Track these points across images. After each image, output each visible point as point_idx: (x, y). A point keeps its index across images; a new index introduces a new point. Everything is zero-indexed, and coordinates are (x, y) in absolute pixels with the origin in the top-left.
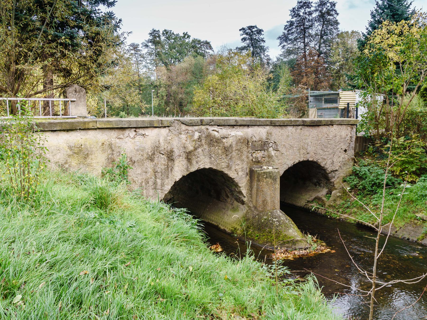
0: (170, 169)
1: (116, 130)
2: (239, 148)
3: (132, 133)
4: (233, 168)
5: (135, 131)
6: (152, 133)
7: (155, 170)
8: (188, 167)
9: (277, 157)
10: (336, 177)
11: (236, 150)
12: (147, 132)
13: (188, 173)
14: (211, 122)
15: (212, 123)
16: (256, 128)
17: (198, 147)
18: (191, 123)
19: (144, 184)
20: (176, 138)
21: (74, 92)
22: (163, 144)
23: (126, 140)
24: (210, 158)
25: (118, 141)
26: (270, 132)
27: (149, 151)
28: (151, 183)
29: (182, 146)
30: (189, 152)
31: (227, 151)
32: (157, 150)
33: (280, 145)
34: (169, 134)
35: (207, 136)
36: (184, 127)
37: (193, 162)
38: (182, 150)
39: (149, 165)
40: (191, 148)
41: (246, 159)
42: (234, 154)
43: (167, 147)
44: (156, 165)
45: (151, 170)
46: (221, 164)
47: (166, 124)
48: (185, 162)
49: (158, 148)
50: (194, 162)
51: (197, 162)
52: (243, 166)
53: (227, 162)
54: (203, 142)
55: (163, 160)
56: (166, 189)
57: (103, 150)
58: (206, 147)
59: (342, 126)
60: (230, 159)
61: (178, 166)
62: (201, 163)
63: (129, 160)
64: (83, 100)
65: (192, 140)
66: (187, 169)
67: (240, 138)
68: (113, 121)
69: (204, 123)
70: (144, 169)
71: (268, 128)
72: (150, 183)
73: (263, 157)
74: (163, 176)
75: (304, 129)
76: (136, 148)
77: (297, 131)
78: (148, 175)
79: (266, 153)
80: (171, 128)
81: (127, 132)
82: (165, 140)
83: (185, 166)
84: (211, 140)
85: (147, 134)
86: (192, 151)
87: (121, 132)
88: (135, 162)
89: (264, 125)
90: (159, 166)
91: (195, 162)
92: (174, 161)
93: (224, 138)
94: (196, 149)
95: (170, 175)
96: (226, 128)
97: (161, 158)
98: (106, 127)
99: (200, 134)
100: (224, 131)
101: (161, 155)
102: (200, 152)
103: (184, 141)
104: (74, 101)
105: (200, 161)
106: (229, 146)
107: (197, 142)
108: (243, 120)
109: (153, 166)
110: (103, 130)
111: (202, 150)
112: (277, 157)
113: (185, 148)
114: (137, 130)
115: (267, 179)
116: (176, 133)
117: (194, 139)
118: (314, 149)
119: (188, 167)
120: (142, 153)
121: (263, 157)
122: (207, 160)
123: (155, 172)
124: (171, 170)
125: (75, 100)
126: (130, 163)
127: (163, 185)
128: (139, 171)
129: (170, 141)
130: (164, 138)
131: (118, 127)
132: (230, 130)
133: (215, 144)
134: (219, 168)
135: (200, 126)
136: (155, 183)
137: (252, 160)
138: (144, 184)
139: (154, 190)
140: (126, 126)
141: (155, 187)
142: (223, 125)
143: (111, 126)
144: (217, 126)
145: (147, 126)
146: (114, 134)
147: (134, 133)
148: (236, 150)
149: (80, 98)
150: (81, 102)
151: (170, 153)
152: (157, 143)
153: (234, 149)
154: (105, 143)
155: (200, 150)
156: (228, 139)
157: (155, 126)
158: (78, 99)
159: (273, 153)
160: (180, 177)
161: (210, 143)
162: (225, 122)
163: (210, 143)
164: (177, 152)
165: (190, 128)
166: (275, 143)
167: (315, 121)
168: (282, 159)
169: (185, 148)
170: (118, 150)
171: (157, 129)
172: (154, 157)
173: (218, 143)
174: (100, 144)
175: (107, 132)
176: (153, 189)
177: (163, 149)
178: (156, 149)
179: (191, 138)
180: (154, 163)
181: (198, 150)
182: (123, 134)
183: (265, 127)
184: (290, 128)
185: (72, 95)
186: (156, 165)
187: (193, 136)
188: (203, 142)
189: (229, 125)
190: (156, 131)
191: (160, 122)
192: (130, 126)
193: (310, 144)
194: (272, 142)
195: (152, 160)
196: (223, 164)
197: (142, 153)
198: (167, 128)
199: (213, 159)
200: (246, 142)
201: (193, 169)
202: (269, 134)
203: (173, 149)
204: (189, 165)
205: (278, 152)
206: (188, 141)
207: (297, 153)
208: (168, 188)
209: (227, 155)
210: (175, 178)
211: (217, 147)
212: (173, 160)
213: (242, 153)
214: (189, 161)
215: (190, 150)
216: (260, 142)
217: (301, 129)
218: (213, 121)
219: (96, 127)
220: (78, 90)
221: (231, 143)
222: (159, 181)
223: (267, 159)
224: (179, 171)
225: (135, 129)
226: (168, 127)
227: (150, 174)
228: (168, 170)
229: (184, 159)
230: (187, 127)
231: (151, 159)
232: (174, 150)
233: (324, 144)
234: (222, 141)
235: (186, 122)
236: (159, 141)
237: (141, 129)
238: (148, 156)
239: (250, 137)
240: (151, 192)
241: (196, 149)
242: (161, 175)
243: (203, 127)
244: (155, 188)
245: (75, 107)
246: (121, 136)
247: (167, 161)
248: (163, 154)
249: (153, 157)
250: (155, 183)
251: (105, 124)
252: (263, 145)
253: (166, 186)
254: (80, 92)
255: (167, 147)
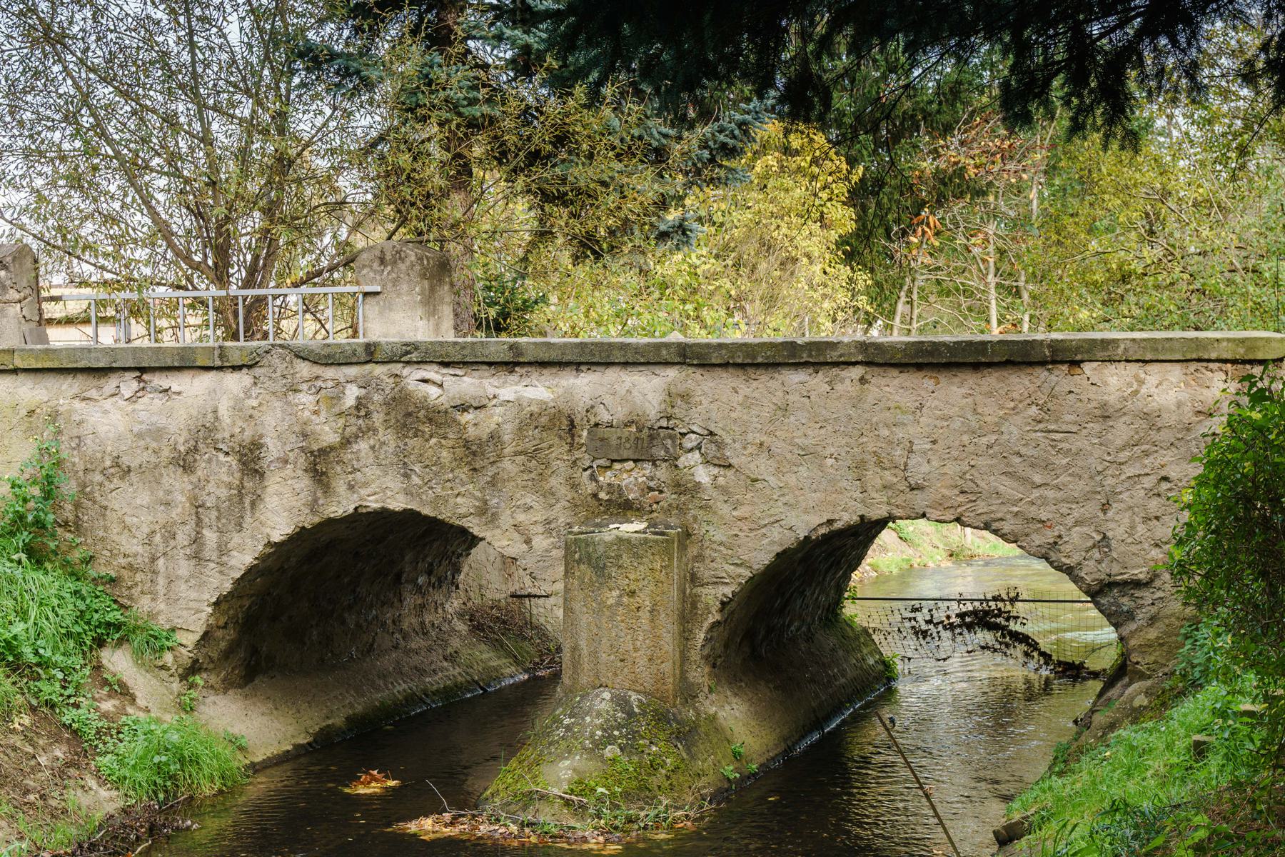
0: (247, 501)
1: (80, 377)
2: (530, 446)
3: (129, 385)
4: (505, 519)
5: (139, 379)
6: (194, 387)
7: (196, 499)
8: (316, 500)
9: (724, 490)
10: (1141, 616)
11: (517, 454)
12: (175, 382)
13: (317, 520)
14: (408, 353)
15: (414, 357)
16: (612, 374)
17: (357, 437)
18: (328, 356)
19: (158, 538)
20: (277, 404)
21: (376, 265)
22: (228, 421)
23: (108, 404)
24: (406, 476)
25: (78, 405)
26: (681, 388)
27: (181, 440)
28: (183, 537)
29: (297, 429)
30: (319, 450)
31: (474, 454)
32: (206, 439)
33: (738, 445)
34: (254, 392)
35: (394, 399)
36: (304, 369)
37: (334, 485)
38: (294, 441)
39: (179, 485)
40: (328, 435)
41: (563, 491)
42: (509, 466)
43: (243, 430)
44: (199, 486)
45: (184, 499)
46: (452, 501)
47: (236, 359)
48: (305, 482)
49: (210, 431)
50: (340, 486)
51: (351, 487)
52: (552, 514)
53: (478, 494)
54: (378, 418)
55: (224, 469)
56: (233, 562)
57: (29, 429)
58: (388, 437)
59: (1150, 367)
60: (492, 483)
61: (279, 494)
62: (369, 491)
63: (108, 463)
64: (405, 287)
65: (336, 410)
66: (313, 506)
67: (534, 408)
68: (61, 350)
69: (378, 357)
70: (161, 494)
71: (672, 373)
72: (180, 537)
73: (651, 489)
74: (224, 521)
75: (883, 382)
76: (136, 430)
77: (839, 387)
78: (175, 513)
79: (663, 473)
80: (257, 371)
81: (111, 383)
82: (237, 408)
83: (305, 497)
84: (410, 414)
85: (175, 388)
86: (332, 448)
87: (91, 381)
88: (129, 471)
89: (648, 363)
90: (211, 487)
91: (345, 487)
92: (262, 475)
93: (464, 408)
94: (349, 442)
95: (248, 519)
96: (476, 374)
97: (219, 463)
98: (39, 366)
99: (363, 391)
100: (467, 385)
101: (221, 457)
102: (363, 454)
103: (307, 413)
104: (378, 293)
105: (366, 484)
106: (485, 437)
107: (353, 420)
108: (549, 345)
109: (190, 487)
110: (40, 376)
111: (372, 448)
112: (724, 490)
113: (305, 436)
114: (145, 377)
115: (582, 567)
116: (278, 387)
117: (344, 408)
118: (952, 469)
119: (316, 500)
120: (154, 445)
121: (651, 489)
122: (393, 482)
123: (198, 507)
124: (253, 504)
125: (378, 289)
126: (112, 470)
127: (223, 550)
128: (144, 498)
129: (255, 413)
130: (232, 403)
131: (75, 366)
132: (494, 381)
133: (427, 429)
134: (445, 514)
135: (368, 367)
136: (197, 540)
137: (595, 496)
138: (158, 538)
139: (193, 562)
140: (101, 365)
141: (196, 553)
142: (465, 363)
143: (56, 365)
144: (435, 367)
145: (169, 364)
146: (70, 386)
147: (135, 385)
148: (517, 454)
149: (395, 282)
150: (399, 295)
151: (251, 450)
152: (210, 416)
153: (509, 450)
154: (38, 411)
155: (363, 446)
156: (481, 414)
157: (198, 364)
158: (389, 285)
159: (703, 475)
160: (289, 530)
161: (405, 425)
162: (465, 352)
163: (405, 425)
164: (273, 448)
165: (330, 373)
166: (711, 433)
167: (944, 344)
168: (752, 504)
169: (305, 436)
170: (75, 432)
171: (212, 374)
172: (195, 461)
173: (439, 425)
174: (24, 412)
175: (52, 382)
176: (189, 558)
177: (227, 435)
178: (205, 434)
179: (333, 406)
180: (194, 479)
181: (355, 447)
182: (99, 388)
183: (657, 370)
184: (794, 378)
185: (372, 275)
186: (199, 486)
187: (339, 398)
188: (378, 418)
189: (490, 364)
190: (205, 381)
191: (217, 353)
192: (114, 365)
193: (922, 445)
194: (695, 428)
195: (187, 468)
196: (459, 500)
197: (154, 445)
198: (245, 370)
199: (415, 480)
200: (565, 424)
201: (341, 505)
202: (674, 397)
203: (261, 436)
204: (319, 494)
205: (730, 473)
206: (323, 414)
207: (844, 484)
208: (243, 558)
209: (475, 470)
210: (268, 530)
211: (434, 441)
212: (261, 474)
213: (548, 465)
214: (320, 481)
215: (325, 444)
216: (634, 429)
217: (862, 380)
218: (416, 349)
219: (11, 367)
220: (388, 257)
221: (493, 426)
222: (210, 536)
223: (669, 497)
224: (281, 513)
225: (138, 374)
226: (249, 367)
227: (179, 510)
228: (241, 502)
229: (300, 473)
230: (318, 370)
231: (185, 463)
232: (267, 440)
233: (1023, 451)
234: (454, 420)
235: (312, 351)
236: (215, 412)
237: (157, 374)
238: (176, 455)
239: (581, 408)
240: (185, 568)
241: (346, 442)
242: (218, 518)
243: (379, 370)
244: (197, 557)
245: (381, 313)
246: (93, 393)
247: (238, 475)
248: (227, 454)
249: (190, 458)
250: (197, 540)
251: (37, 359)
252: (650, 441)
253: (234, 553)
254: (395, 262)
255: (243, 430)
